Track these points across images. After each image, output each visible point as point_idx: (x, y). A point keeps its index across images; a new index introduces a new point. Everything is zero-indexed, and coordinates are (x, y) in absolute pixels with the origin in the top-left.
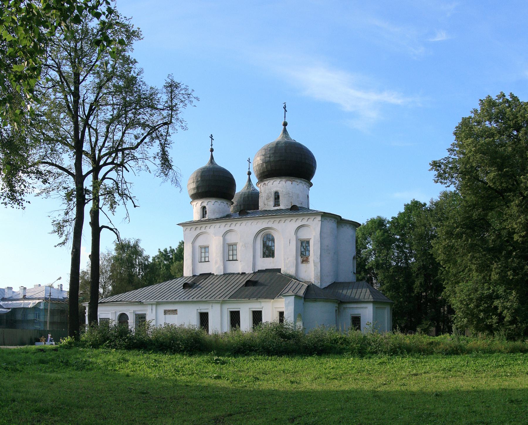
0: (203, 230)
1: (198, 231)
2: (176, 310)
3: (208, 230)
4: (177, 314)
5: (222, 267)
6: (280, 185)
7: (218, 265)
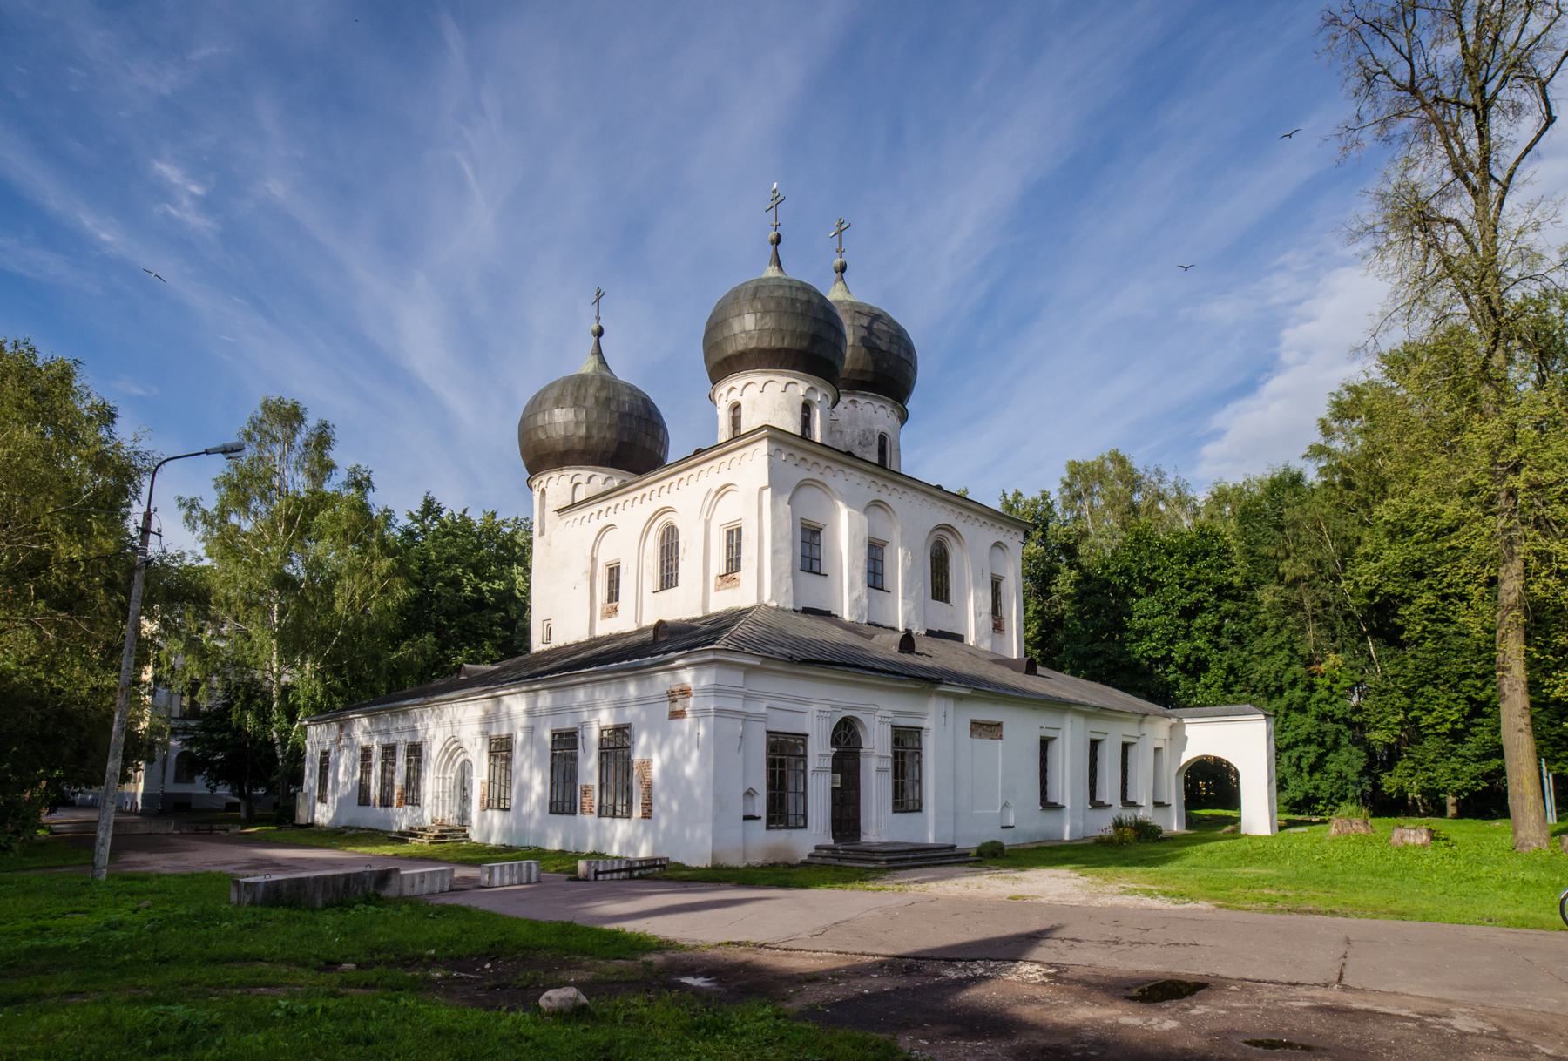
0: (815, 474)
1: (801, 474)
2: (999, 725)
3: (828, 479)
4: (1001, 737)
5: (865, 601)
6: (889, 421)
7: (856, 594)
